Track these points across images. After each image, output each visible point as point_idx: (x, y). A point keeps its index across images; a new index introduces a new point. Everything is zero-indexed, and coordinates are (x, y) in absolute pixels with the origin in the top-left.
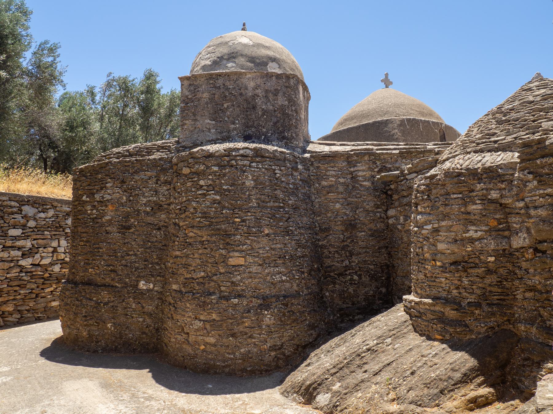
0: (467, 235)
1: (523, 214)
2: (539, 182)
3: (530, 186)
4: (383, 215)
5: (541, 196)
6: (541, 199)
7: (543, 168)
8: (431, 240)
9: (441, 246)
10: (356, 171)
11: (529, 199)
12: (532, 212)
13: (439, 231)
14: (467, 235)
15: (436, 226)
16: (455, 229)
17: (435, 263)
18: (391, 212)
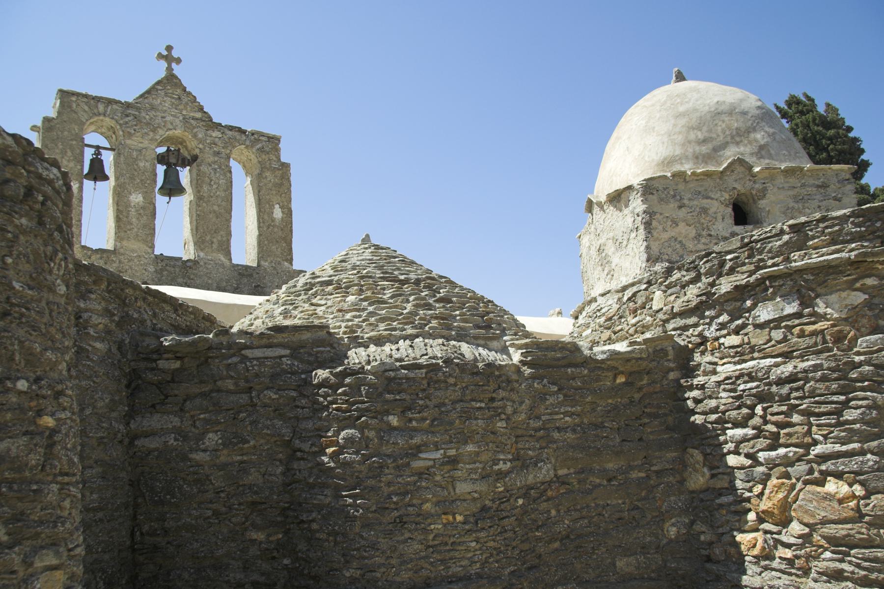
0: (496, 468)
1: (542, 438)
2: (565, 396)
3: (551, 400)
4: (121, 427)
5: (566, 414)
6: (567, 419)
7: (574, 379)
8: (438, 478)
9: (463, 488)
10: (86, 311)
11: (548, 417)
12: (556, 435)
13: (458, 463)
14: (496, 468)
15: (452, 452)
16: (484, 457)
17: (455, 518)
18: (154, 421)
